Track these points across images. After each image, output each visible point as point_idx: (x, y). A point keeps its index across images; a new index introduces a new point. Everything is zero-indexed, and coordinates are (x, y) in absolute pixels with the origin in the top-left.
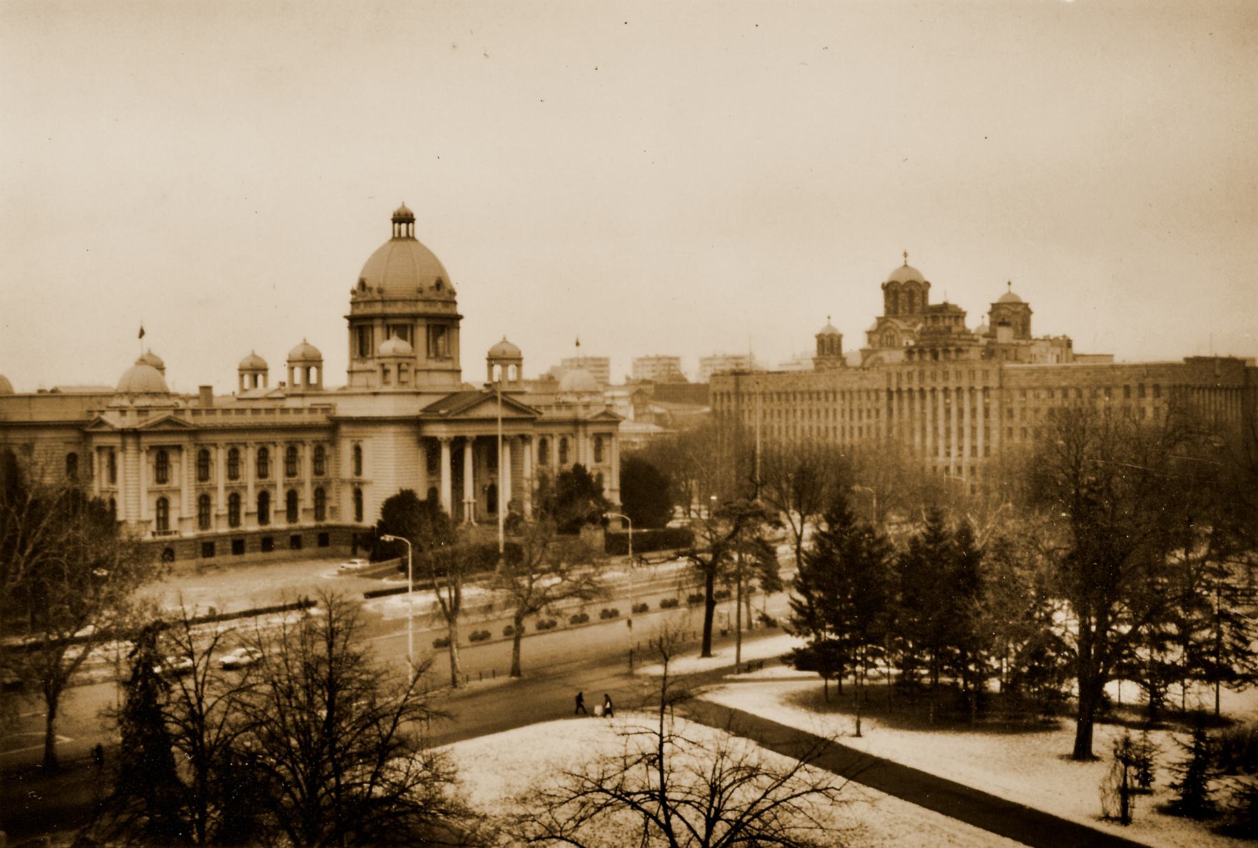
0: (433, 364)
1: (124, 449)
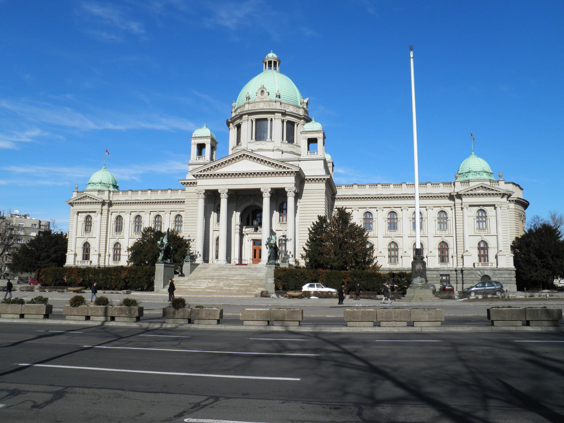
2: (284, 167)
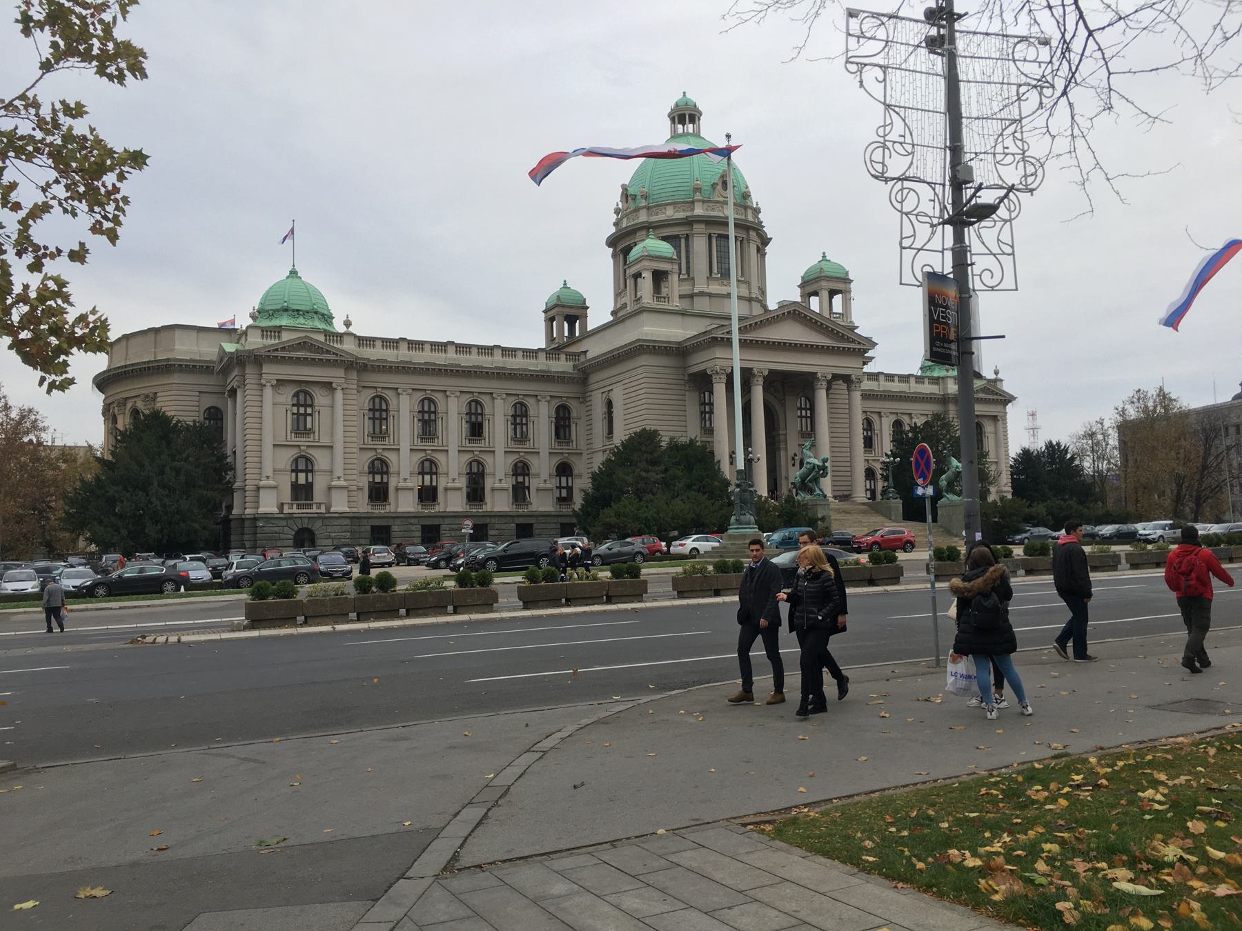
0: (715, 288)
1: (243, 384)
2: (854, 341)
